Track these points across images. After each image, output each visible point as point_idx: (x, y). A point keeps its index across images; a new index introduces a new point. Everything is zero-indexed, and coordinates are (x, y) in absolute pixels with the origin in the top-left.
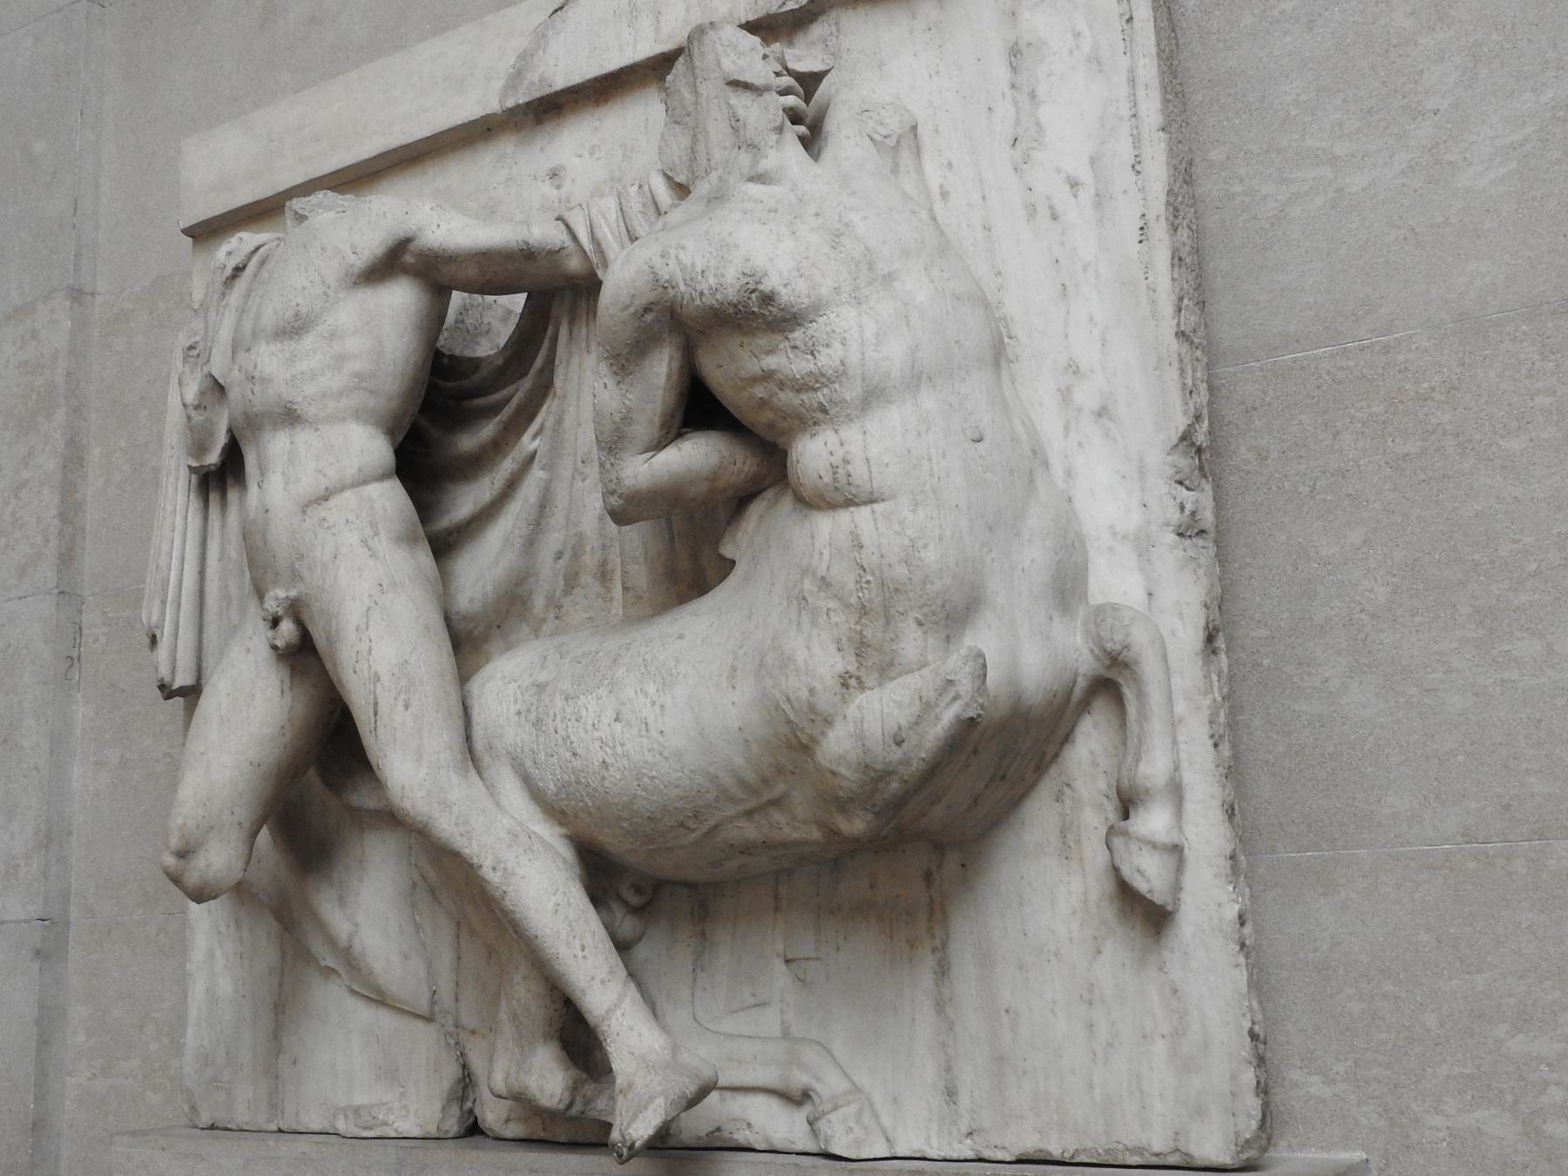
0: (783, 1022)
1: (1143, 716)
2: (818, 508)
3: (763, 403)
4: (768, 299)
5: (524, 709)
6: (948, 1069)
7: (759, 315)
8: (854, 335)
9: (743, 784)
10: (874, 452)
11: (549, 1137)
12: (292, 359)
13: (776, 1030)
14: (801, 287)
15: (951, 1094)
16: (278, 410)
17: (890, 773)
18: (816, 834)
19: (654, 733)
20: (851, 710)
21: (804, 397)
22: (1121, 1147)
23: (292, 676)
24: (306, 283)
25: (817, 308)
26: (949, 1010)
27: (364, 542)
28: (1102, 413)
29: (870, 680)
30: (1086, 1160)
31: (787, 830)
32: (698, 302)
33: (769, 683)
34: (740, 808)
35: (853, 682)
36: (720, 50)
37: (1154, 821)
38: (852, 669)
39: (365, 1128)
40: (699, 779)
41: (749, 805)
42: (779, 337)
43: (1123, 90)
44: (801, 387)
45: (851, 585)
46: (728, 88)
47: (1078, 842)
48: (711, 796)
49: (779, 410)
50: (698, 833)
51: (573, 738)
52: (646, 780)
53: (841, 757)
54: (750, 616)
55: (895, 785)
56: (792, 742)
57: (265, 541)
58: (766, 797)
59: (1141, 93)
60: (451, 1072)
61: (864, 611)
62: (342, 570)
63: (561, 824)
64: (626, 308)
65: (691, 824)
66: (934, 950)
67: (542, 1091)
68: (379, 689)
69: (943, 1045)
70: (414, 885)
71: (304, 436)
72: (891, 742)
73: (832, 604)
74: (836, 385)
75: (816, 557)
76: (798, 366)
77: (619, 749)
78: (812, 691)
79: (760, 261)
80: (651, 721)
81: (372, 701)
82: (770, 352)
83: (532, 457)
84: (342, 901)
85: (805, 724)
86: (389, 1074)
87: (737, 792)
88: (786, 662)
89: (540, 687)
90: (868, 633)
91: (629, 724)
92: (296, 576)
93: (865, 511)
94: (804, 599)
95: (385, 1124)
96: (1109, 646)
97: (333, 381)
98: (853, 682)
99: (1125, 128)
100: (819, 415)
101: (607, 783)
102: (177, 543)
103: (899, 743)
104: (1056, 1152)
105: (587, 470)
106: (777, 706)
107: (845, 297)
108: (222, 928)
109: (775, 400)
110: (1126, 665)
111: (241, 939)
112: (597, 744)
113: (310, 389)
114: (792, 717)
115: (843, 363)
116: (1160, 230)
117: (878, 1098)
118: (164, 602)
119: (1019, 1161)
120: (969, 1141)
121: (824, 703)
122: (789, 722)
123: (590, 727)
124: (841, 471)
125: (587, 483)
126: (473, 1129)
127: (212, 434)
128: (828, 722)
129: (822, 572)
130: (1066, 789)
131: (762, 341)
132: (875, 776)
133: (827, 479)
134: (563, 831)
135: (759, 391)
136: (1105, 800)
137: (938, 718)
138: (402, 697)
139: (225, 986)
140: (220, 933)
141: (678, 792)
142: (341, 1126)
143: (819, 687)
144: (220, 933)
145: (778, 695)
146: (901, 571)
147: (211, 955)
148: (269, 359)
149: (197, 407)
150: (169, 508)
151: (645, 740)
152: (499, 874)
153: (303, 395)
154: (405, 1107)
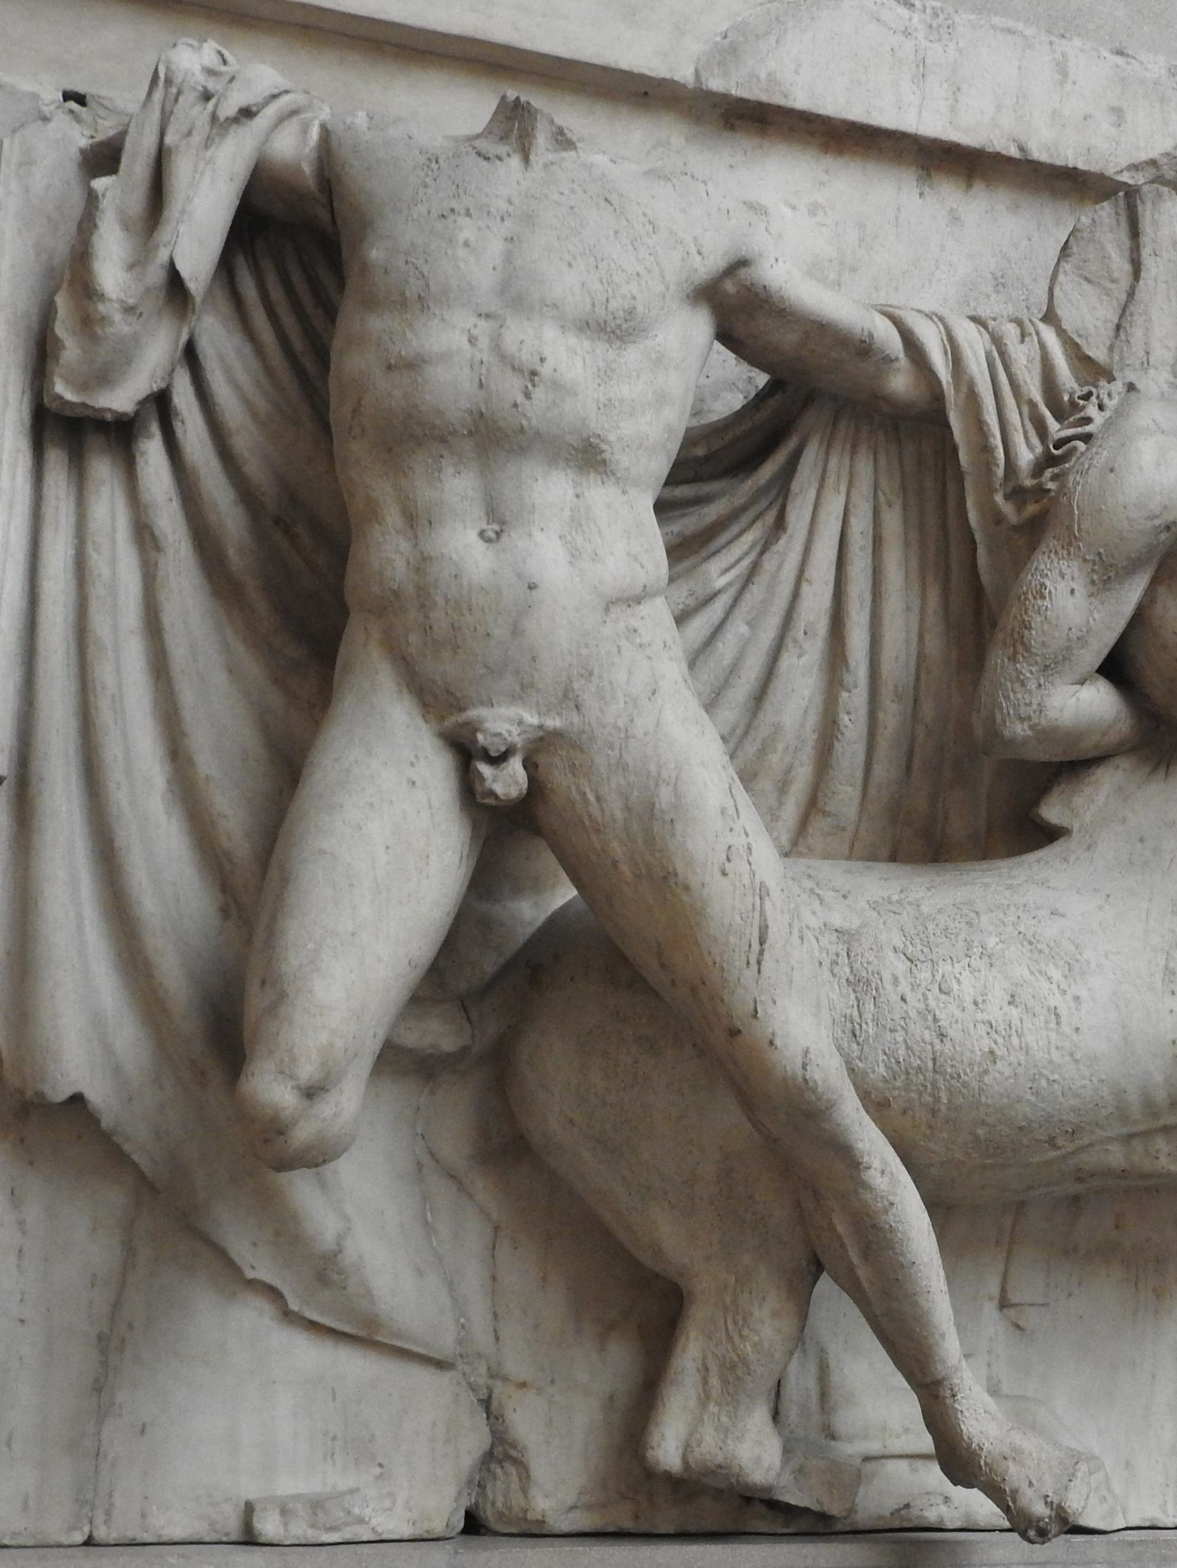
9: (1149, 1106)
11: (644, 1527)
12: (606, 374)
16: (569, 439)
19: (1066, 1029)
23: (472, 838)
24: (640, 269)
31: (1163, 1160)
34: (1125, 1130)
39: (332, 1529)
40: (1105, 1091)
41: (1134, 1129)
50: (1063, 1151)
52: (1044, 1083)
57: (516, 631)
65: (1060, 1142)
68: (768, 905)
71: (600, 495)
77: (1015, 1040)
80: (1063, 1011)
81: (757, 922)
83: (719, 592)
86: (358, 1447)
87: (1136, 1111)
92: (569, 698)
101: (986, 1079)
105: (807, 645)
112: (983, 1029)
113: (628, 428)
123: (970, 1007)
125: (803, 660)
138: (796, 931)
141: (1073, 1102)
148: (566, 356)
151: (1053, 1035)
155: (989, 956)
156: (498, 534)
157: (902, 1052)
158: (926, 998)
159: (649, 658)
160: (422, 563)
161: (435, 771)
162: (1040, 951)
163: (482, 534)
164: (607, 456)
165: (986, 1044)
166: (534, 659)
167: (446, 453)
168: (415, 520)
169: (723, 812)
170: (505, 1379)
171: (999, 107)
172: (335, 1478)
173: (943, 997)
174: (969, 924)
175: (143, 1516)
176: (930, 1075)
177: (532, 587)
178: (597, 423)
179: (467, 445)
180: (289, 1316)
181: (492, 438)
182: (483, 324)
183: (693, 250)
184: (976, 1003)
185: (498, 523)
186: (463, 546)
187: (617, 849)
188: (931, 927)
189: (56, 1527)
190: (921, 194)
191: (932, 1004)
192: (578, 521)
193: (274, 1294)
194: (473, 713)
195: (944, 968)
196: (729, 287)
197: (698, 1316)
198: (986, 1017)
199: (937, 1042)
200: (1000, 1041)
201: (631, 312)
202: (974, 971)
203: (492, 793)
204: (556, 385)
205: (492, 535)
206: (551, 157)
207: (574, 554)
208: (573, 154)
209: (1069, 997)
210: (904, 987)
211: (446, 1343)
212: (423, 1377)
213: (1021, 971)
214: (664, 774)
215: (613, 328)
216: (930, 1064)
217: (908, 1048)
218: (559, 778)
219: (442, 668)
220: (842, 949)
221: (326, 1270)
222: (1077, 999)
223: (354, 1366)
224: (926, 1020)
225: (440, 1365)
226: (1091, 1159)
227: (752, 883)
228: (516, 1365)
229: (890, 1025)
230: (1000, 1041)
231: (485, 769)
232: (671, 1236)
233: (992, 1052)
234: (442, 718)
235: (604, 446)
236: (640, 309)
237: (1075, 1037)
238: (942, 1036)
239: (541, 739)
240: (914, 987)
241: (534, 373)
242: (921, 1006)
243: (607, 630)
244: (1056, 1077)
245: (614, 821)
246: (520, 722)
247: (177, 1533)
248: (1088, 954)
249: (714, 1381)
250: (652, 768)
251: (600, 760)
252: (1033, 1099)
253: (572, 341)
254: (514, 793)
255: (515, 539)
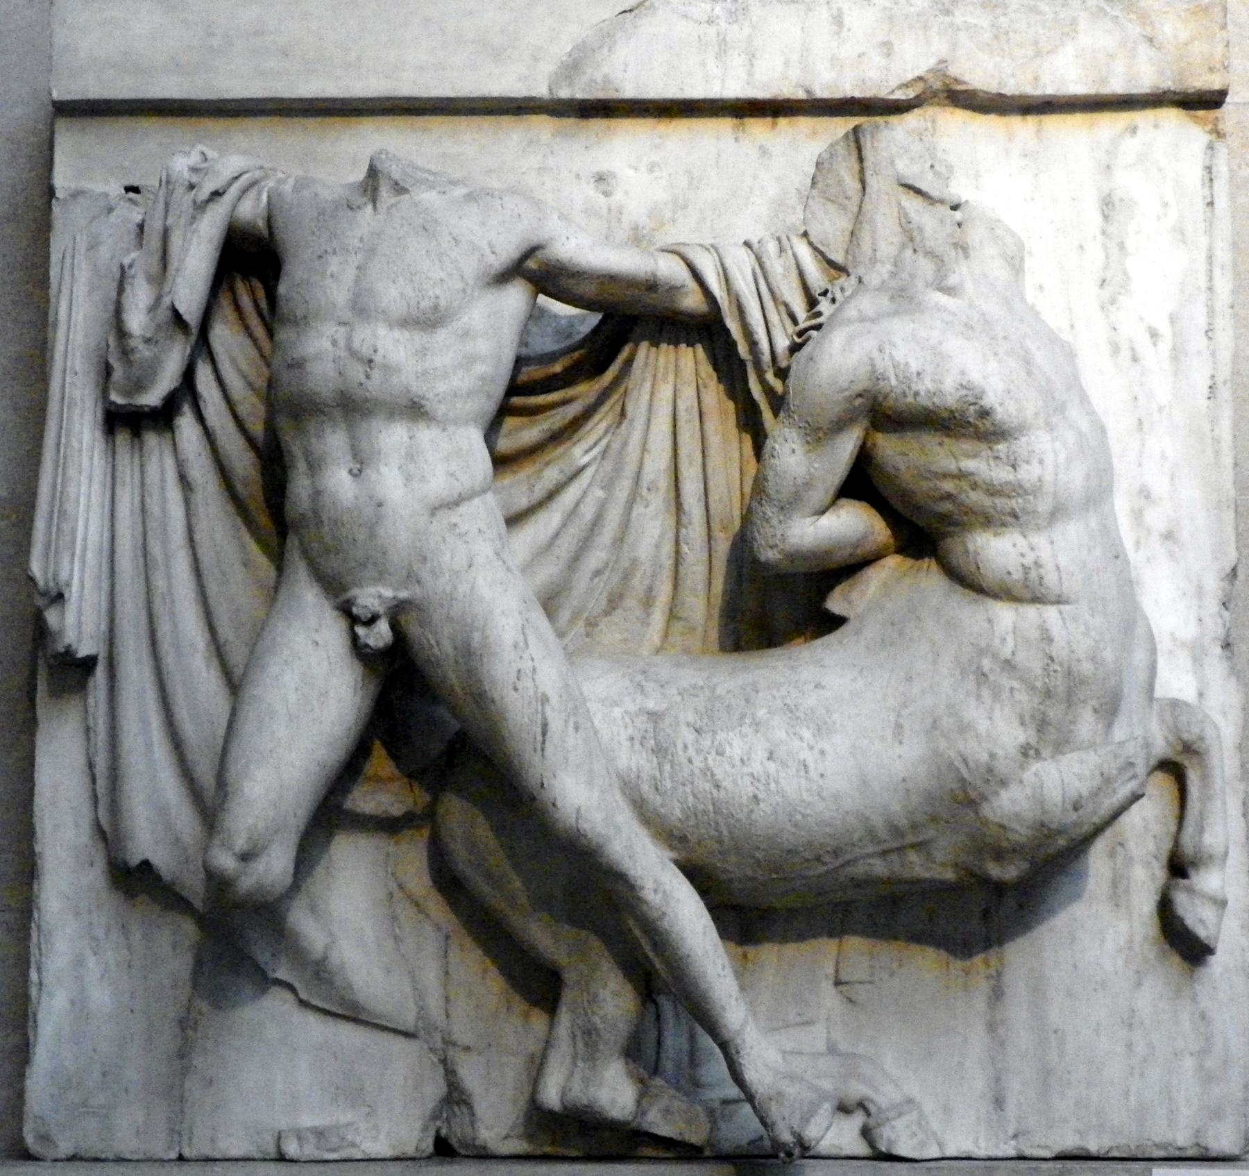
0: (828, 1039)
1: (1206, 798)
2: (996, 596)
3: (949, 496)
4: (985, 413)
5: (638, 737)
6: (998, 1080)
7: (966, 423)
8: (1046, 459)
9: (896, 831)
10: (1063, 561)
12: (423, 352)
13: (821, 1046)
14: (1012, 408)
15: (999, 1102)
17: (1060, 832)
18: (949, 875)
19: (813, 774)
20: (1028, 776)
21: (997, 501)
22: (1150, 1143)
25: (1021, 429)
26: (1001, 1031)
27: (497, 554)
28: (1169, 536)
29: (1046, 753)
30: (1115, 1154)
32: (910, 399)
33: (943, 744)
34: (878, 849)
35: (1032, 752)
36: (894, 150)
37: (1208, 880)
38: (1033, 742)
40: (851, 819)
41: (886, 846)
42: (984, 446)
43: (1201, 265)
44: (994, 491)
45: (1039, 671)
46: (901, 189)
47: (1127, 891)
48: (856, 836)
49: (961, 504)
51: (716, 771)
53: (1017, 815)
54: (909, 679)
55: (1062, 842)
56: (959, 797)
57: (372, 536)
58: (910, 839)
59: (1217, 272)
60: (435, 1089)
61: (1048, 694)
62: (480, 581)
63: (672, 848)
64: (843, 391)
65: (827, 858)
66: (988, 977)
67: (613, 1101)
69: (992, 1059)
70: (391, 894)
71: (426, 435)
72: (1069, 807)
73: (1016, 684)
74: (1031, 498)
75: (997, 641)
76: (1001, 474)
77: (773, 785)
78: (992, 756)
79: (975, 376)
82: (968, 456)
84: (313, 909)
85: (979, 783)
88: (964, 728)
89: (654, 717)
90: (1051, 714)
91: (784, 764)
92: (412, 577)
93: (1051, 612)
94: (984, 674)
95: (353, 1145)
96: (1185, 736)
97: (461, 381)
98: (1032, 752)
99: (1203, 298)
100: (1009, 519)
102: (84, 489)
103: (1076, 809)
104: (1093, 1147)
106: (951, 764)
107: (1041, 421)
108: (100, 933)
109: (963, 497)
110: (1197, 753)
111: (129, 947)
112: (748, 780)
113: (442, 387)
114: (966, 775)
115: (1040, 480)
116: (1225, 393)
117: (928, 1106)
118: (73, 555)
119: (1057, 1158)
120: (1013, 1142)
121: (1002, 767)
122: (962, 781)
123: (738, 763)
124: (1033, 575)
126: (444, 1149)
127: (155, 374)
128: (1003, 783)
129: (1006, 652)
130: (1119, 849)
131: (967, 445)
132: (1045, 832)
133: (1017, 575)
134: (674, 855)
135: (948, 486)
136: (1154, 861)
137: (1114, 791)
139: (100, 996)
140: (94, 939)
142: (291, 1149)
143: (1000, 753)
144: (94, 939)
145: (952, 754)
146: (1087, 667)
147: (79, 962)
149: (148, 341)
150: (75, 444)
151: (803, 781)
152: (659, 896)
153: (435, 391)
154: (376, 1127)
155: (757, 724)
156: (360, 471)
157: (691, 799)
158: (706, 759)
159: (467, 542)
160: (317, 494)
161: (333, 633)
162: (798, 718)
163: (350, 471)
164: (427, 408)
165: (751, 790)
166: (384, 553)
167: (324, 418)
168: (315, 467)
169: (516, 646)
170: (454, 1044)
171: (787, 63)
172: (346, 1117)
173: (719, 758)
174: (747, 701)
175: (213, 1141)
176: (712, 815)
177: (380, 505)
178: (418, 388)
179: (337, 413)
180: (303, 1004)
181: (352, 407)
182: (342, 329)
183: (488, 251)
184: (742, 761)
185: (361, 463)
186: (340, 483)
187: (451, 675)
188: (717, 705)
189: (159, 1147)
190: (736, 140)
191: (710, 762)
192: (411, 455)
193: (290, 987)
194: (354, 592)
195: (721, 736)
196: (531, 264)
197: (568, 996)
198: (750, 770)
199: (715, 792)
200: (762, 788)
201: (436, 308)
202: (743, 736)
203: (367, 646)
204: (387, 368)
205: (355, 471)
206: (393, 200)
207: (408, 479)
208: (407, 196)
209: (816, 751)
210: (691, 752)
211: (408, 1019)
212: (399, 1043)
213: (781, 734)
214: (476, 624)
215: (427, 320)
216: (711, 808)
217: (694, 796)
218: (414, 630)
219: (332, 564)
220: (650, 726)
221: (320, 971)
222: (822, 753)
223: (348, 1035)
224: (705, 775)
225: (407, 1035)
226: (860, 870)
227: (536, 693)
228: (462, 1034)
229: (681, 780)
230: (762, 788)
231: (361, 631)
232: (545, 937)
233: (755, 797)
234: (336, 597)
235: (423, 402)
236: (443, 303)
237: (821, 782)
238: (718, 786)
239: (396, 606)
240: (698, 751)
241: (371, 361)
242: (702, 765)
243: (435, 527)
244: (808, 811)
245: (447, 655)
246: (380, 597)
247: (235, 1152)
248: (836, 716)
249: (579, 1038)
250: (469, 620)
251: (436, 617)
252: (794, 830)
253: (397, 333)
254: (381, 644)
255: (370, 473)
